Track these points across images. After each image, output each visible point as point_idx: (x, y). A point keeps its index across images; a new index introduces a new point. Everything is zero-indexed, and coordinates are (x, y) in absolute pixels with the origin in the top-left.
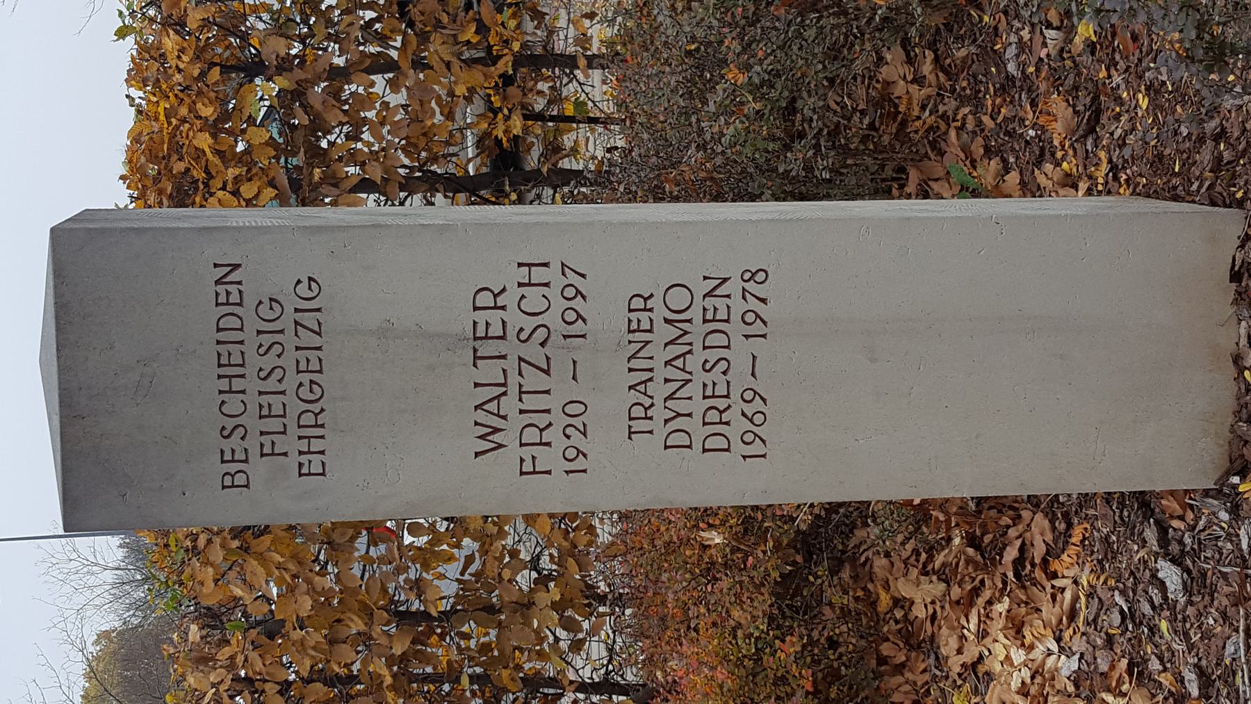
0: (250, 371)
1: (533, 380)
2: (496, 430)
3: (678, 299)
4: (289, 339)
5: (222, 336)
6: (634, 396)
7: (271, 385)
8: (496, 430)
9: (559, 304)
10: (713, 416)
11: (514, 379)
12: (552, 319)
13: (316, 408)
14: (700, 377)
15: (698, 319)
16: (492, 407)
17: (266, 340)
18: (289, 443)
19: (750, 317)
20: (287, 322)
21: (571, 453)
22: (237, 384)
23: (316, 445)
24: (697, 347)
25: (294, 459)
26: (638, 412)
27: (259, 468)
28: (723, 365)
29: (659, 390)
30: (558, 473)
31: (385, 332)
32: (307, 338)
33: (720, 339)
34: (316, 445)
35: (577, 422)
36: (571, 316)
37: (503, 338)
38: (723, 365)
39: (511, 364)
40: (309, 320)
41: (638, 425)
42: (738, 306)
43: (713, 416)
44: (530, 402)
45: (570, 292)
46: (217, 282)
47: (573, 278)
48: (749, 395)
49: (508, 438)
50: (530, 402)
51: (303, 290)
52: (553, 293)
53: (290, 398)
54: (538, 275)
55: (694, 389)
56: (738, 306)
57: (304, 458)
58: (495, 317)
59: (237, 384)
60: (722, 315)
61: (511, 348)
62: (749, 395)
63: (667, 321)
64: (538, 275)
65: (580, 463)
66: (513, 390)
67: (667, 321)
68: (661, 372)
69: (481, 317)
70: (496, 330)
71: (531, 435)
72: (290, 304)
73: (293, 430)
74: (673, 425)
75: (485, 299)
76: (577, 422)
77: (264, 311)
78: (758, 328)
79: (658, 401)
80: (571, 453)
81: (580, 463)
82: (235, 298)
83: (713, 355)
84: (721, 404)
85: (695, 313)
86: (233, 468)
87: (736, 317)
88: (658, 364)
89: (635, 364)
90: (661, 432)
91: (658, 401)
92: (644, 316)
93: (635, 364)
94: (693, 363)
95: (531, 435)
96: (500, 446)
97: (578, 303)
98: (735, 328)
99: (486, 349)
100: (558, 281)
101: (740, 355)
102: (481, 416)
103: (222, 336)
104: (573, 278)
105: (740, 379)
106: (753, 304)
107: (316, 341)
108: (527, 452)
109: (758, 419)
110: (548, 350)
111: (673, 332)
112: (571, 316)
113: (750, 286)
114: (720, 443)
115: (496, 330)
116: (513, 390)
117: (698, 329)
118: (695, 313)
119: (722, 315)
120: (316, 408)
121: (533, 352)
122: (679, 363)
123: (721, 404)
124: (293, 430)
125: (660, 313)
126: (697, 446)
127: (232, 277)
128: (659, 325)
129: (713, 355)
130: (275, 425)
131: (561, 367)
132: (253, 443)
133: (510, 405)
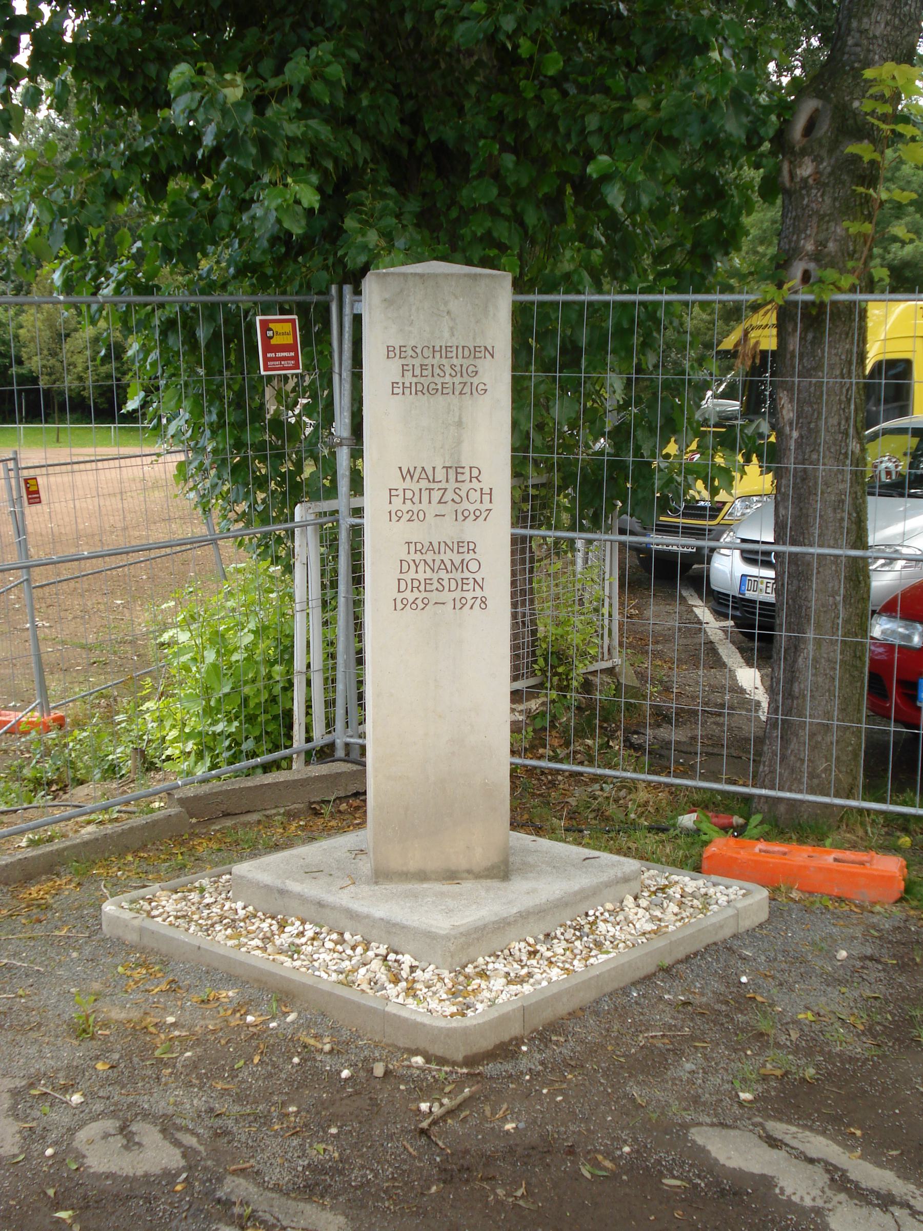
0: (444, 361)
1: (436, 495)
2: (412, 478)
3: (473, 566)
4: (457, 380)
5: (460, 350)
6: (427, 545)
7: (437, 371)
8: (412, 478)
9: (472, 508)
10: (416, 584)
11: (436, 486)
12: (465, 505)
13: (425, 391)
14: (435, 577)
15: (464, 576)
16: (424, 476)
17: (458, 369)
18: (409, 379)
19: (464, 601)
20: (466, 378)
21: (399, 514)
22: (438, 355)
23: (407, 391)
24: (450, 575)
25: (400, 380)
26: (419, 547)
27: (396, 365)
28: (441, 588)
29: (429, 557)
30: (389, 507)
31: (460, 424)
32: (458, 387)
33: (453, 587)
34: (407, 391)
35: (415, 517)
36: (466, 513)
37: (457, 481)
38: (441, 588)
39: (443, 485)
40: (467, 389)
41: (412, 547)
42: (469, 595)
43: (416, 584)
44: (425, 494)
45: (478, 513)
46: (486, 348)
47: (484, 514)
48: (426, 601)
49: (408, 483)
50: (425, 494)
51: (481, 387)
52: (477, 505)
53: (430, 379)
54: (486, 498)
55: (429, 574)
56: (469, 595)
57: (400, 385)
58: (467, 477)
59: (438, 355)
60: (465, 587)
61: (452, 485)
62: (426, 601)
63: (463, 560)
64: (486, 498)
65: (394, 518)
66: (432, 486)
67: (463, 560)
68: (438, 558)
69: (467, 471)
70: (460, 478)
71: (409, 494)
72: (475, 381)
73: (414, 380)
74: (412, 564)
75: (475, 473)
76: (415, 517)
77: (471, 369)
78: (458, 605)
79: (424, 557)
80: (399, 514)
81: (394, 518)
82: (478, 355)
83: (445, 583)
84: (422, 588)
85: (466, 574)
86: (397, 352)
87: (465, 594)
88: (442, 556)
89: (443, 545)
90: (409, 558)
91: (424, 557)
92: (466, 549)
93: (443, 545)
94: (443, 574)
95: (409, 494)
96: (404, 479)
97: (472, 517)
98: (458, 594)
99: (452, 473)
100: (483, 508)
101: (447, 596)
102: (419, 470)
103: (460, 350)
104: (484, 514)
105: (434, 596)
106: (470, 603)
107: (457, 393)
108: (401, 492)
109: (414, 606)
110: (450, 503)
111: (457, 563)
112: (466, 513)
113: (479, 601)
114: (403, 588)
115: (460, 478)
116: (432, 486)
117: (459, 576)
118: (466, 574)
119: (465, 587)
120: (425, 391)
121: (449, 495)
122: (442, 566)
123: (422, 588)
124: (414, 380)
125: (467, 557)
126: (402, 576)
127: (487, 354)
128: (461, 557)
129: (445, 583)
130: (417, 372)
131: (442, 509)
132: (410, 361)
133: (424, 484)
